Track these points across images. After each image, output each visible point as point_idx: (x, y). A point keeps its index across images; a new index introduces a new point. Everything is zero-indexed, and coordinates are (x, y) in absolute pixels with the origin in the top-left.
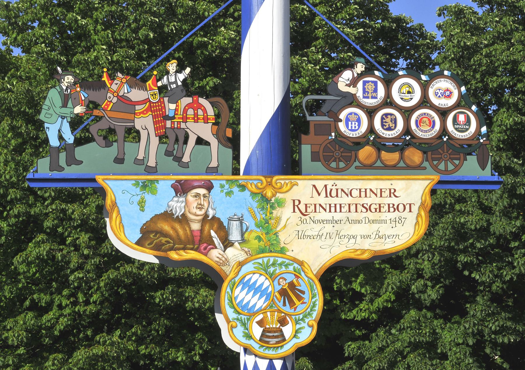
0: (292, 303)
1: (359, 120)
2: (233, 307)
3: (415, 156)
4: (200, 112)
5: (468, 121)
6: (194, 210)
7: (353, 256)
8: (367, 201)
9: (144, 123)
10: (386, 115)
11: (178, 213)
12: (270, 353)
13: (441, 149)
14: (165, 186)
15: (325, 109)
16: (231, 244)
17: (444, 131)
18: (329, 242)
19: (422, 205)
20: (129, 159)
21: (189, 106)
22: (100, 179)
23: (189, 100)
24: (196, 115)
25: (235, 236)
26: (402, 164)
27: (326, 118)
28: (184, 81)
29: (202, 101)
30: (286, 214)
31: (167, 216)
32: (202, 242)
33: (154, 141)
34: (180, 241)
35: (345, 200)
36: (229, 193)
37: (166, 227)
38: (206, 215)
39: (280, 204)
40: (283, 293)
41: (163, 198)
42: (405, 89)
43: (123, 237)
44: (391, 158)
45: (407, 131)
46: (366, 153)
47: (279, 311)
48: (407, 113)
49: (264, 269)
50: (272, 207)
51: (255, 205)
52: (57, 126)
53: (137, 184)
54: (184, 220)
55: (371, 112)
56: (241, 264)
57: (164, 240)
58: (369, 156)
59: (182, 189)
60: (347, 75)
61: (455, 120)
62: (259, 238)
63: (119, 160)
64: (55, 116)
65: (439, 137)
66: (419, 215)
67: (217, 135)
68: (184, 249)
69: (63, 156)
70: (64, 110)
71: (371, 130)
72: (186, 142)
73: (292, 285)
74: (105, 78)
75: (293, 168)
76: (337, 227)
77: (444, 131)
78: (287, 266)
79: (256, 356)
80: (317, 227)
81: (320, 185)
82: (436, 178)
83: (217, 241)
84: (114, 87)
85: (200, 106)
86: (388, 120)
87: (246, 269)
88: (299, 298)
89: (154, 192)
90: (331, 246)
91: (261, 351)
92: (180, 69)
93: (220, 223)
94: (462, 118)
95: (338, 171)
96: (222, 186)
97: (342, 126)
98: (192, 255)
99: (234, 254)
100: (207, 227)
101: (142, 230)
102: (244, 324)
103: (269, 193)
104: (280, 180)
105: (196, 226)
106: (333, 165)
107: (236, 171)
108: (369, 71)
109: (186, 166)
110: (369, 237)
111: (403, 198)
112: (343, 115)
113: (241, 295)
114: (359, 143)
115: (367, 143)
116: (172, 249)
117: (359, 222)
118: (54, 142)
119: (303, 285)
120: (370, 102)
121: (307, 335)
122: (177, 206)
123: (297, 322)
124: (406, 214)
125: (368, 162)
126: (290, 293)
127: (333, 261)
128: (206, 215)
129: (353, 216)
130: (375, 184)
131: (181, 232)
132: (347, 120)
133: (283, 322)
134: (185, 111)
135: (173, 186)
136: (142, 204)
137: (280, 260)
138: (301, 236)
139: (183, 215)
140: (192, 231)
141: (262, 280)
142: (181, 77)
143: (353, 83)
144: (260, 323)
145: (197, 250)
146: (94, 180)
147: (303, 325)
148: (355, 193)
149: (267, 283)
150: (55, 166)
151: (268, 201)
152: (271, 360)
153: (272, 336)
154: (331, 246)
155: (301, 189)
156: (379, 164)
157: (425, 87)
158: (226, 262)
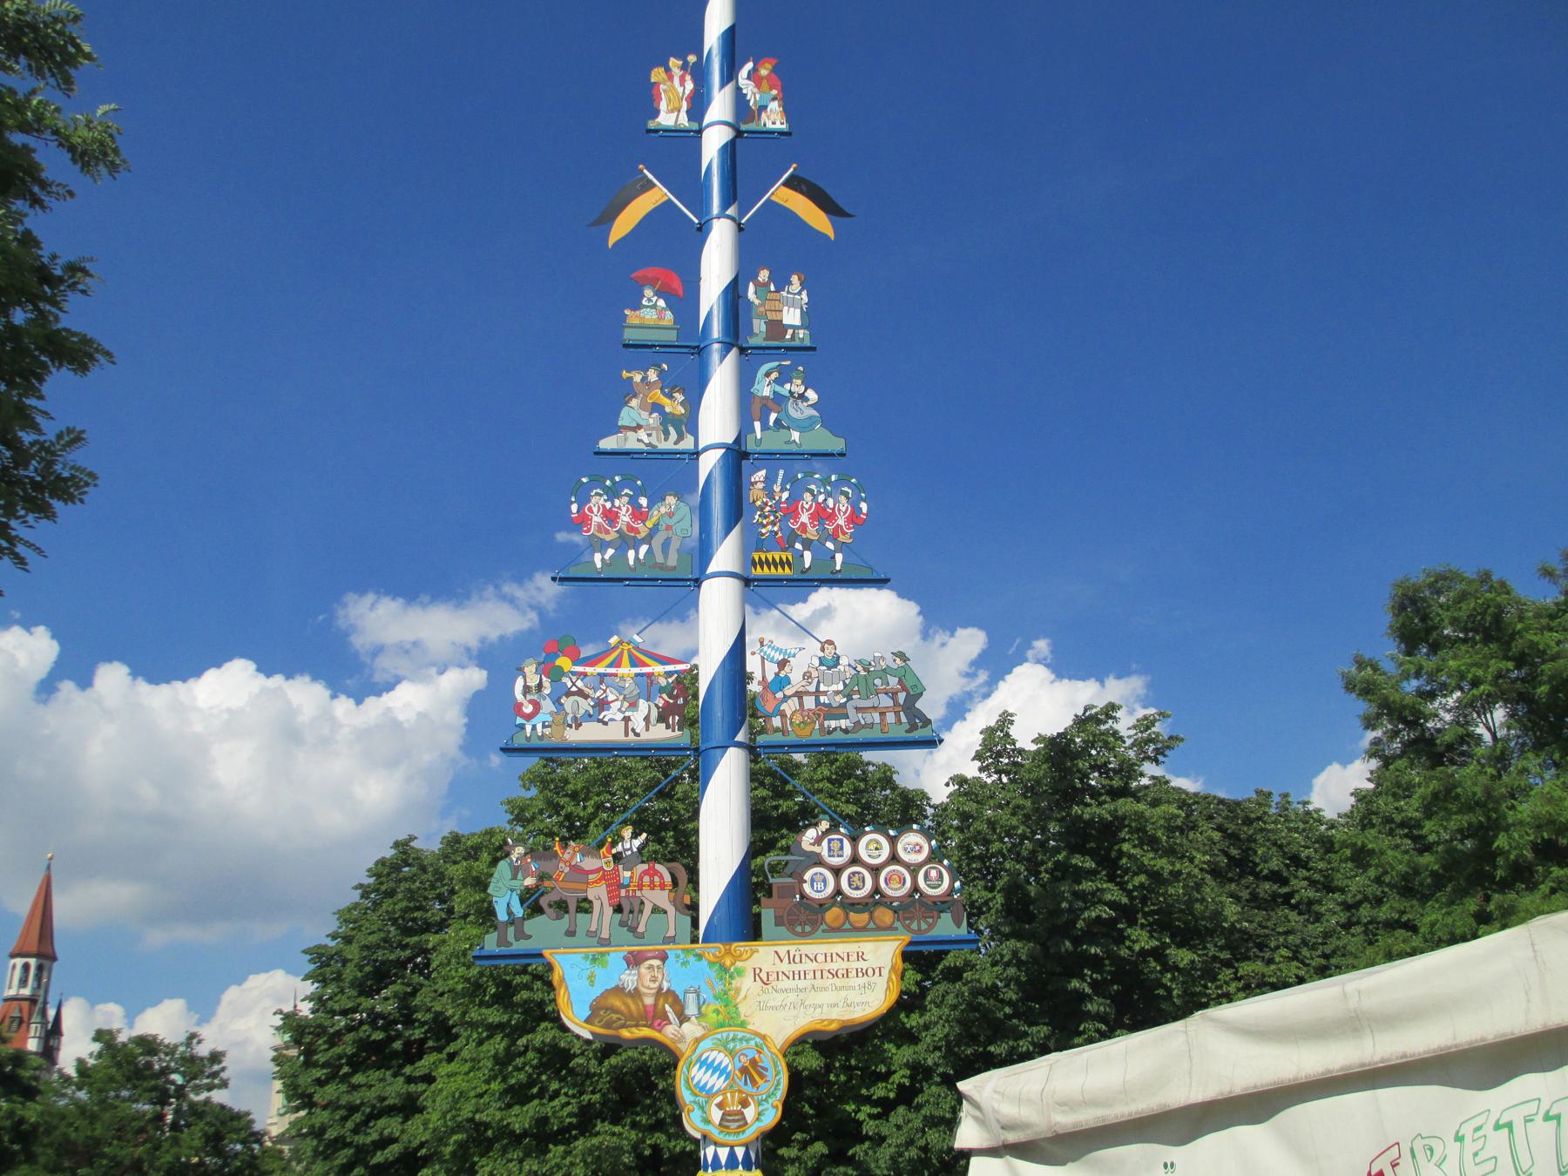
0: (754, 1082)
1: (825, 881)
2: (689, 1088)
3: (885, 916)
4: (656, 879)
6: (648, 984)
7: (819, 1027)
8: (834, 966)
9: (598, 893)
10: (854, 873)
11: (631, 987)
12: (731, 1139)
13: (915, 906)
14: (616, 957)
15: (788, 870)
16: (688, 1019)
17: (916, 888)
18: (794, 1013)
19: (893, 968)
20: (580, 932)
21: (645, 873)
22: (546, 953)
23: (646, 866)
24: (652, 882)
25: (691, 1009)
26: (872, 925)
27: (790, 880)
28: (640, 849)
29: (658, 867)
30: (746, 984)
31: (618, 990)
32: (655, 1017)
33: (609, 910)
34: (632, 1017)
35: (809, 966)
36: (685, 963)
37: (617, 1003)
38: (660, 988)
39: (740, 973)
40: (744, 1070)
41: (616, 972)
42: (872, 847)
43: (576, 1017)
44: (860, 918)
45: (876, 890)
46: (833, 914)
47: (740, 1092)
48: (875, 870)
49: (723, 1046)
50: (731, 977)
51: (713, 974)
52: (506, 899)
53: (586, 958)
54: (636, 994)
55: (837, 872)
56: (698, 1041)
57: (615, 1016)
58: (837, 918)
59: (634, 960)
60: (811, 834)
62: (717, 1012)
63: (571, 933)
64: (504, 890)
65: (910, 895)
66: (890, 979)
67: (674, 902)
68: (637, 1026)
69: (511, 930)
70: (514, 883)
71: (838, 891)
72: (641, 912)
73: (753, 1062)
74: (557, 848)
75: (753, 931)
76: (802, 995)
77: (916, 889)
78: (748, 1041)
79: (716, 1144)
80: (781, 997)
81: (782, 950)
82: (907, 938)
83: (672, 1016)
84: (567, 856)
85: (657, 873)
86: (856, 878)
87: (703, 1045)
88: (762, 1076)
89: (604, 965)
90: (796, 1017)
91: (720, 1137)
92: (635, 835)
93: (676, 997)
94: (933, 873)
95: (803, 935)
96: (678, 956)
97: (807, 888)
98: (645, 1032)
99: (691, 1029)
100: (661, 1001)
101: (591, 1007)
102: (702, 1108)
103: (728, 963)
104: (740, 947)
105: (649, 1001)
106: (799, 929)
107: (694, 940)
108: (834, 827)
109: (642, 936)
110: (836, 1005)
111: (871, 962)
112: (807, 876)
113: (699, 1075)
114: (822, 906)
115: (833, 905)
116: (623, 1026)
117: (825, 989)
118: (502, 916)
119: (766, 1061)
120: (836, 861)
121: (771, 1117)
122: (629, 979)
123: (759, 1103)
124: (876, 978)
125: (836, 924)
126: (751, 1072)
127: (798, 1034)
128: (660, 988)
129: (818, 982)
130: (841, 948)
131: (633, 1007)
132: (813, 881)
133: (745, 1104)
134: (641, 878)
135: (625, 958)
136: (591, 979)
137: (740, 1035)
138: (762, 1006)
139: (636, 989)
140: (645, 1006)
141: (721, 1058)
142: (637, 843)
143: (818, 841)
144: (720, 1106)
145: (651, 1026)
146: (541, 955)
147: (766, 1106)
148: (821, 958)
149: (726, 1061)
150: (502, 941)
151: (726, 970)
152: (732, 1147)
153: (733, 1119)
154: (796, 1017)
155: (763, 955)
156: (847, 926)
157: (893, 841)
158: (682, 1038)
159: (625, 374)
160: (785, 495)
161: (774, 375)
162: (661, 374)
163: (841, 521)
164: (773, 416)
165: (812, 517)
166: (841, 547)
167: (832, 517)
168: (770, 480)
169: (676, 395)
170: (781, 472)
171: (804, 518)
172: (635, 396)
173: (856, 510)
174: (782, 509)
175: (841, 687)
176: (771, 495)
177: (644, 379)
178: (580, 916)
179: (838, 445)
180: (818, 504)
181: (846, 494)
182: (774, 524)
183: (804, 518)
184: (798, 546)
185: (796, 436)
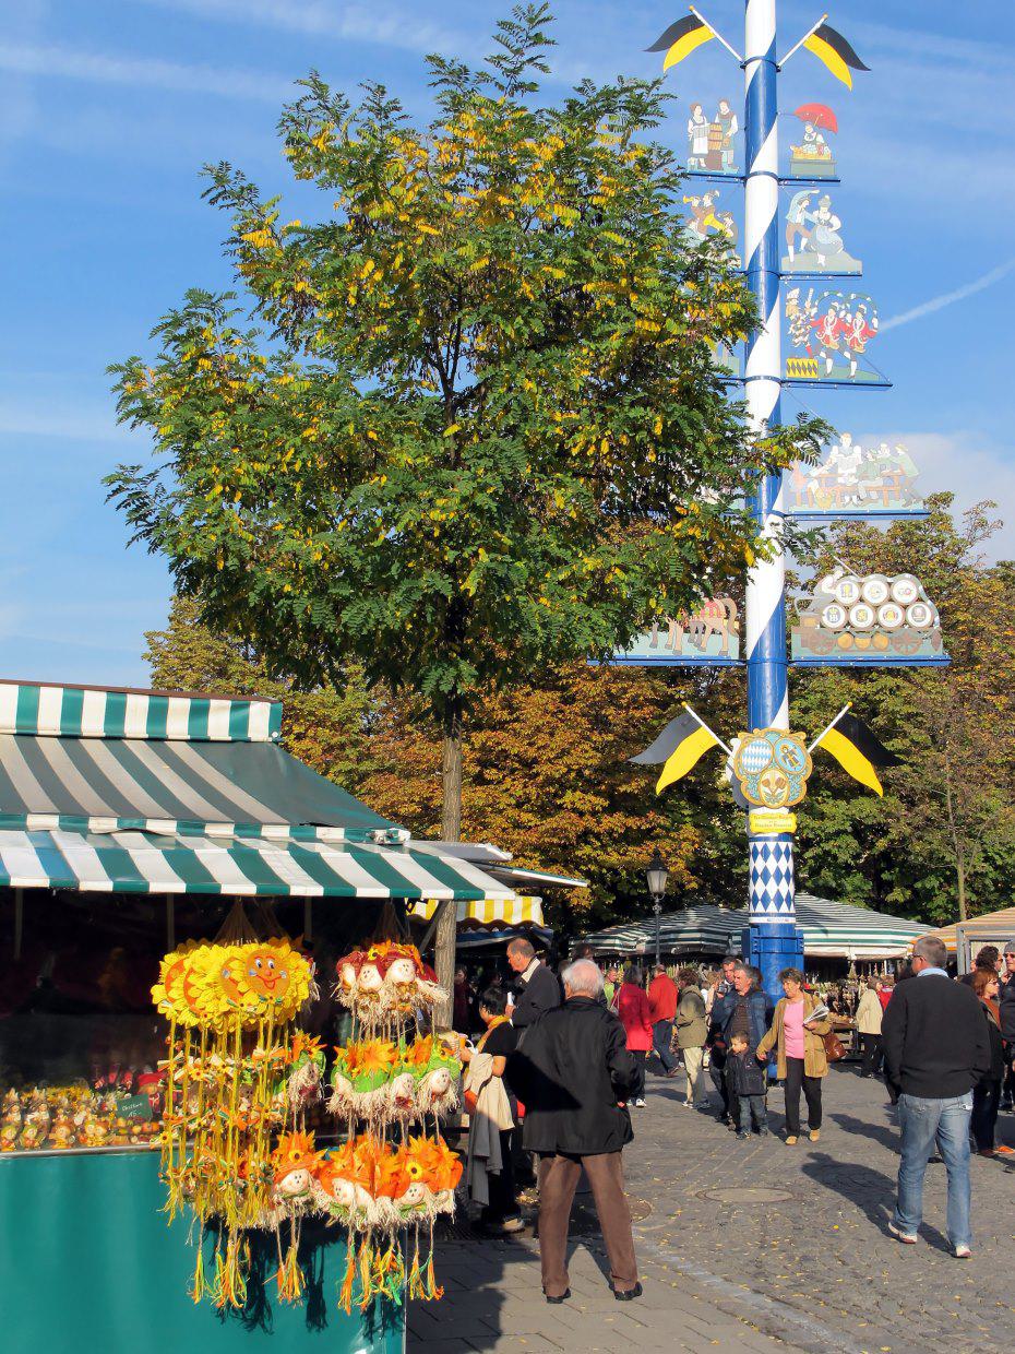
1: (838, 613)
5: (924, 613)
15: (811, 607)
48: (876, 608)
61: (913, 613)
94: (919, 611)
112: (825, 612)
143: (834, 586)
159: (685, 200)
160: (814, 311)
161: (806, 203)
162: (715, 200)
163: (857, 334)
164: (804, 242)
165: (834, 332)
166: (855, 356)
167: (850, 330)
168: (802, 299)
169: (727, 219)
170: (812, 291)
171: (828, 331)
172: (694, 219)
173: (868, 323)
174: (811, 323)
175: (854, 470)
176: (802, 311)
177: (701, 204)
178: (660, 634)
179: (854, 265)
180: (839, 319)
181: (861, 311)
182: (804, 335)
183: (828, 331)
184: (823, 354)
185: (822, 259)
